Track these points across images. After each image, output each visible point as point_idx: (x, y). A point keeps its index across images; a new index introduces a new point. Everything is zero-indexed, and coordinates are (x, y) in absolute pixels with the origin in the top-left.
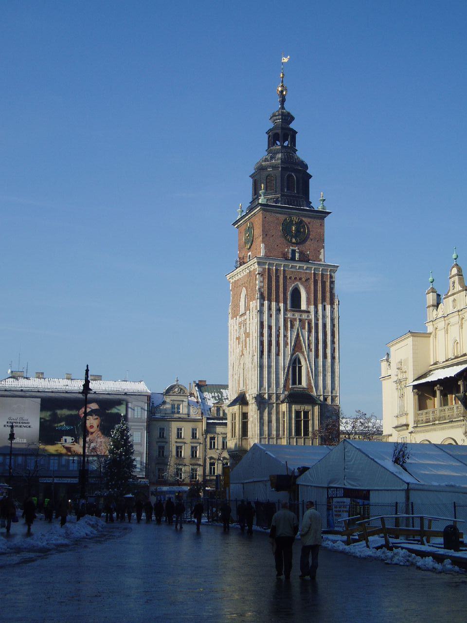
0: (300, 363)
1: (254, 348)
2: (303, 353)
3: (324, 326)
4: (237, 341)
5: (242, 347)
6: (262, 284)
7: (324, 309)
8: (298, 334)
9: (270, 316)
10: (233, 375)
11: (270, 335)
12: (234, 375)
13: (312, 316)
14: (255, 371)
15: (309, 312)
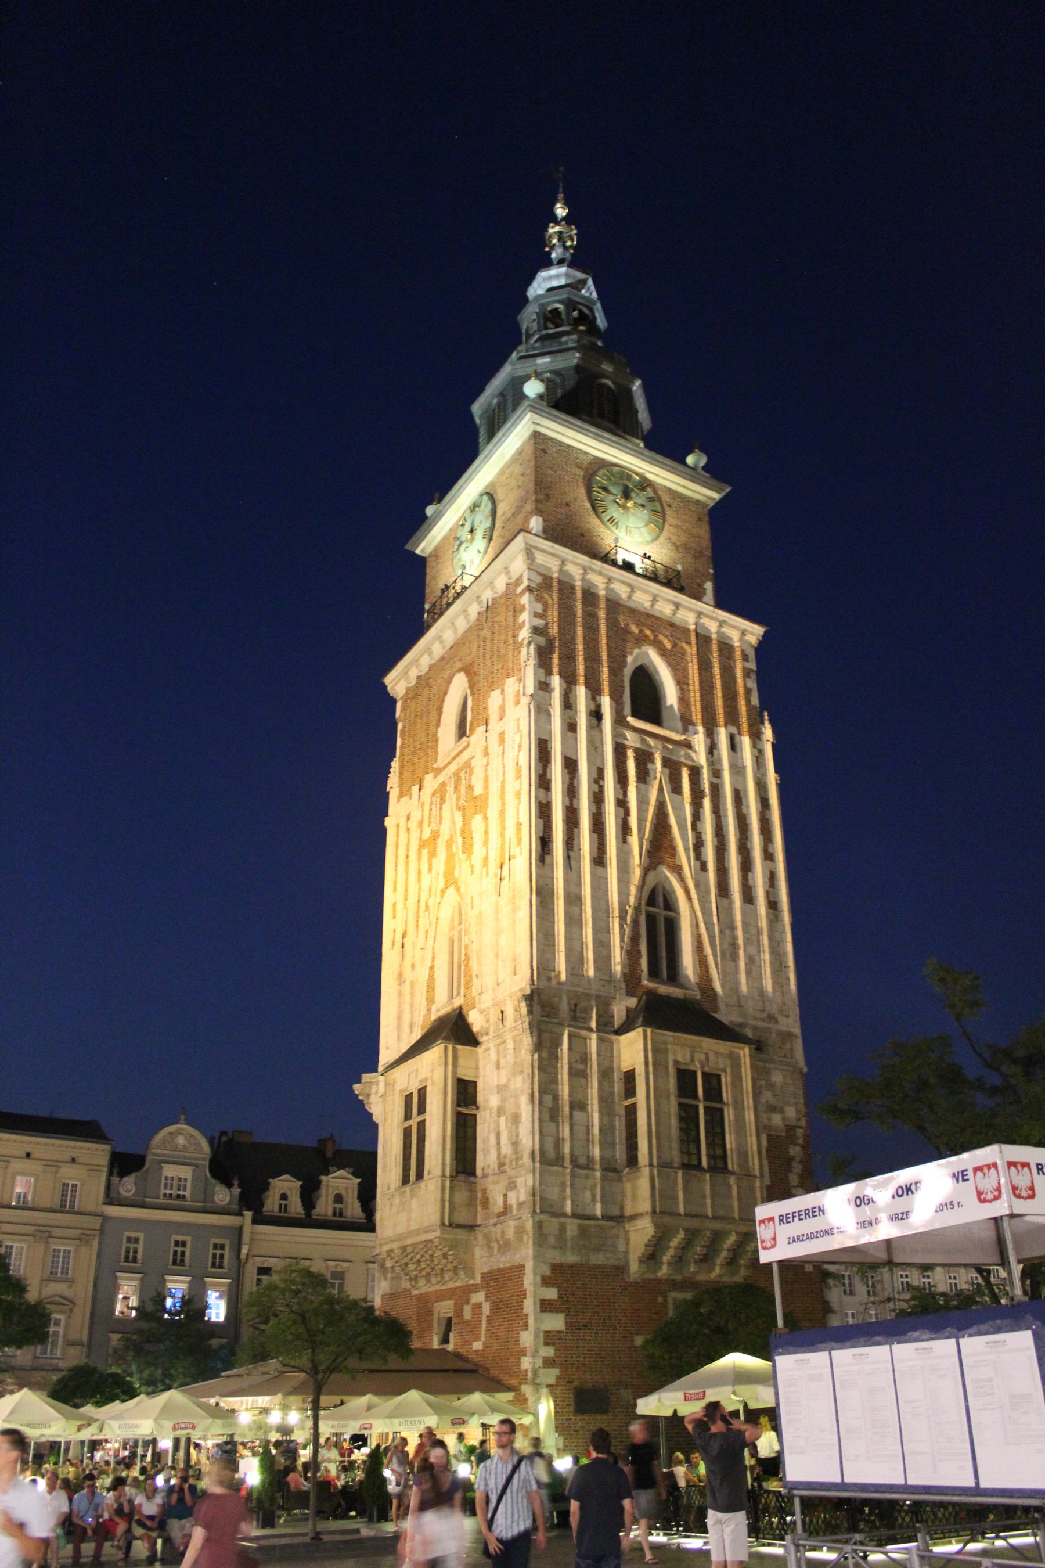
0: (670, 905)
1: (510, 832)
2: (678, 870)
3: (739, 798)
4: (425, 852)
5: (451, 857)
6: (539, 622)
7: (733, 746)
8: (661, 807)
9: (571, 727)
10: (400, 975)
11: (571, 791)
12: (408, 975)
13: (701, 757)
14: (515, 910)
15: (688, 745)
